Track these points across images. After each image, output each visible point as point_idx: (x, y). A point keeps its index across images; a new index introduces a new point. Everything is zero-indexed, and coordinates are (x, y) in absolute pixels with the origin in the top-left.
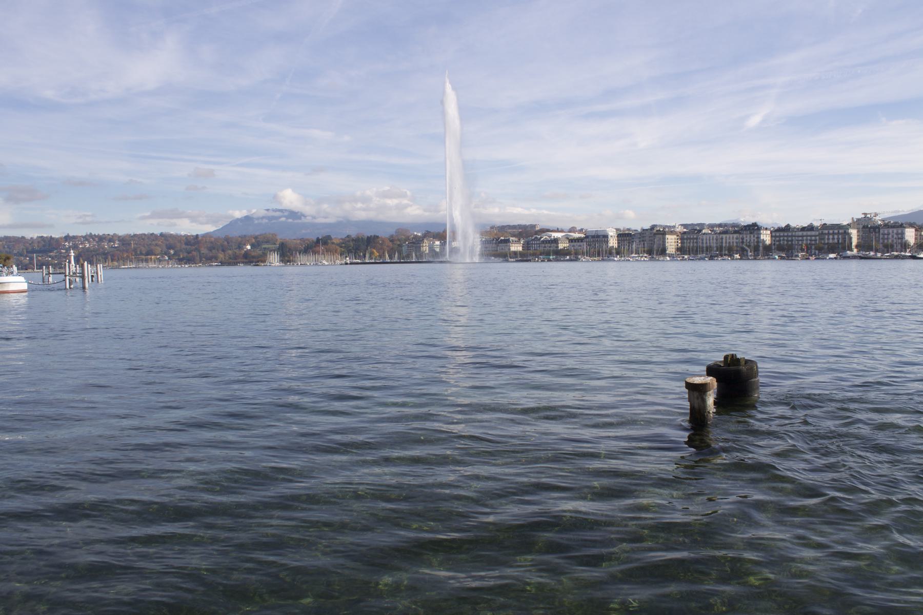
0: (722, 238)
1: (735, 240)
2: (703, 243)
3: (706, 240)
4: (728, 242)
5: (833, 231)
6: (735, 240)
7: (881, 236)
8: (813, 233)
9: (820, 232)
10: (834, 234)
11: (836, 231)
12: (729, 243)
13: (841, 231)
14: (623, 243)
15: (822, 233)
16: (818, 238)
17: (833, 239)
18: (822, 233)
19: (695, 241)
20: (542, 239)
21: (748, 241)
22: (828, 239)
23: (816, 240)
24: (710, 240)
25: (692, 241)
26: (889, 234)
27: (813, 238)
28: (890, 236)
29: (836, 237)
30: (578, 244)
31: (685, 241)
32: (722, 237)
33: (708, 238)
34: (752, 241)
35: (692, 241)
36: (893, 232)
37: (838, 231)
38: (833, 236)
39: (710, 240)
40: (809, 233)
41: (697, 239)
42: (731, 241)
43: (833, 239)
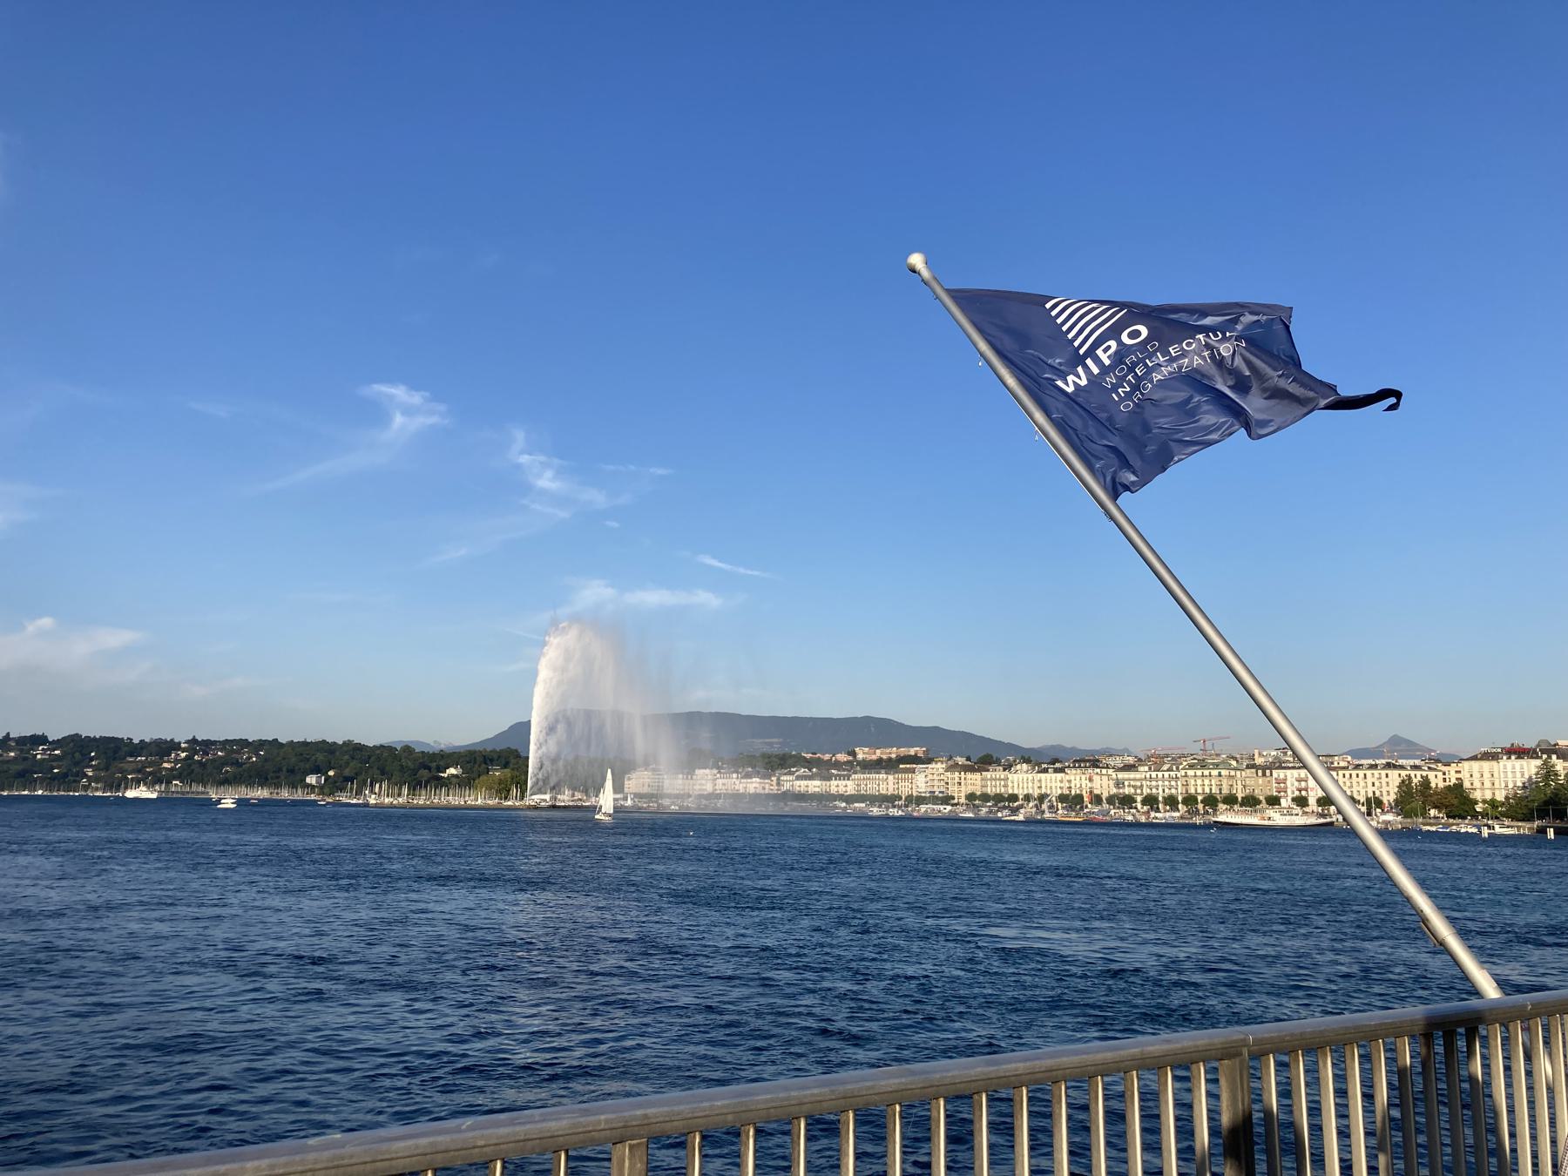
0: (1040, 781)
1: (1059, 784)
4: (1048, 787)
6: (1059, 784)
12: (1051, 788)
14: (903, 784)
19: (1003, 783)
20: (797, 773)
21: (1078, 786)
25: (998, 783)
29: (1207, 782)
30: (844, 783)
31: (989, 783)
33: (1020, 780)
34: (1084, 786)
35: (998, 783)
41: (1006, 779)
42: (1054, 785)
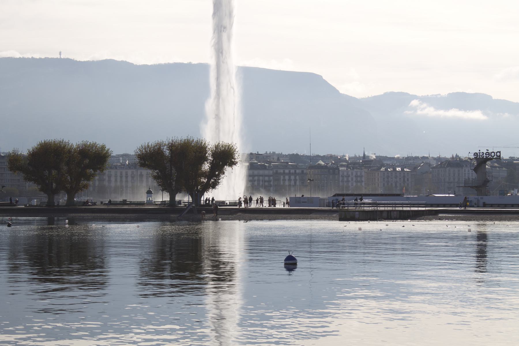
2: (109, 181)
3: (116, 176)
5: (290, 171)
7: (341, 179)
8: (266, 172)
9: (275, 171)
10: (290, 174)
11: (292, 171)
13: (298, 171)
15: (277, 173)
16: (271, 178)
17: (290, 180)
18: (277, 173)
22: (284, 180)
23: (269, 181)
24: (121, 177)
26: (349, 176)
27: (267, 178)
28: (354, 179)
29: (293, 177)
32: (141, 173)
36: (352, 174)
37: (295, 171)
38: (290, 177)
39: (121, 177)
40: (261, 172)
43: (290, 180)
